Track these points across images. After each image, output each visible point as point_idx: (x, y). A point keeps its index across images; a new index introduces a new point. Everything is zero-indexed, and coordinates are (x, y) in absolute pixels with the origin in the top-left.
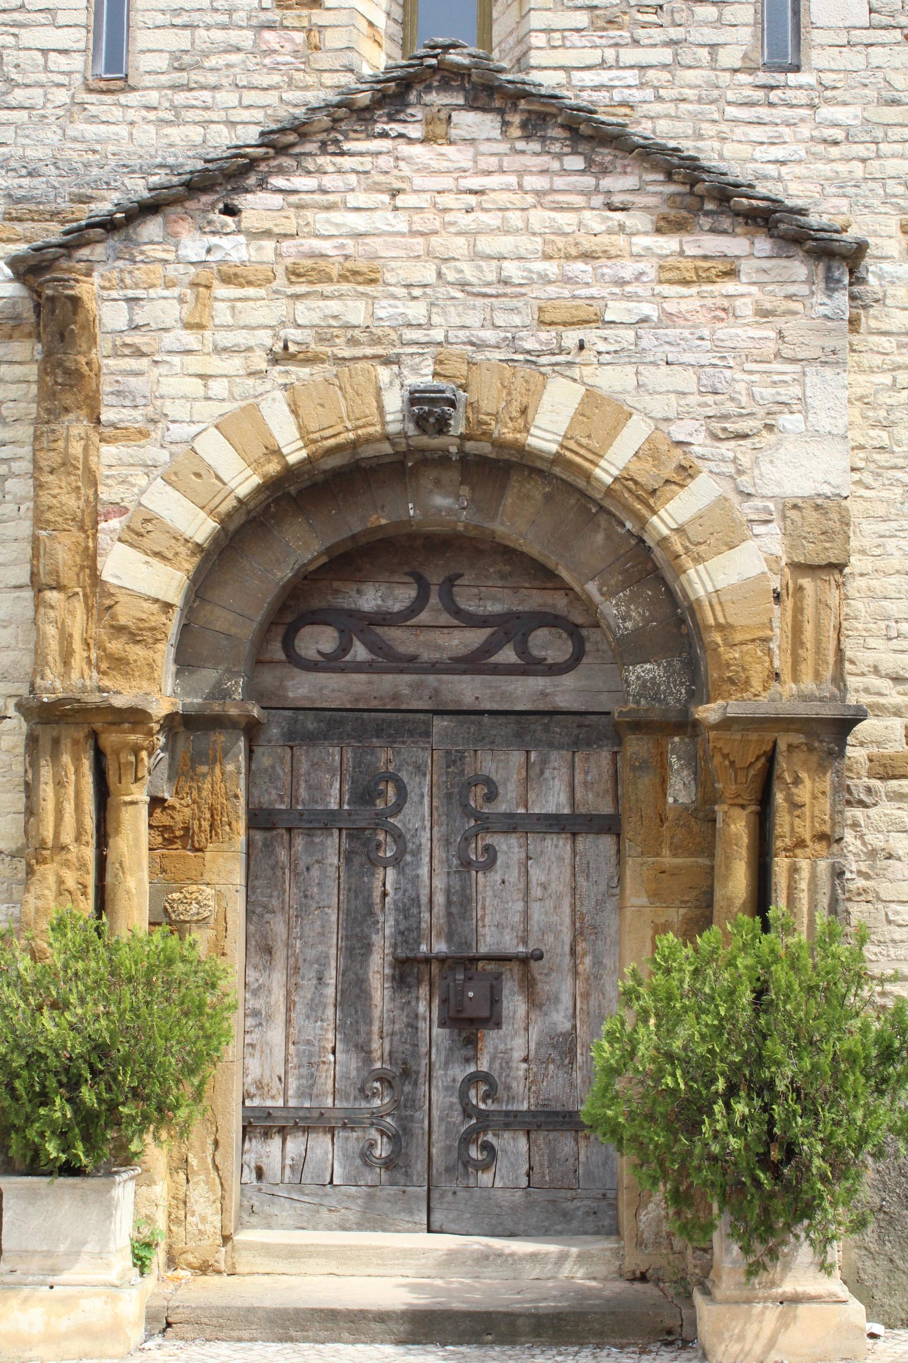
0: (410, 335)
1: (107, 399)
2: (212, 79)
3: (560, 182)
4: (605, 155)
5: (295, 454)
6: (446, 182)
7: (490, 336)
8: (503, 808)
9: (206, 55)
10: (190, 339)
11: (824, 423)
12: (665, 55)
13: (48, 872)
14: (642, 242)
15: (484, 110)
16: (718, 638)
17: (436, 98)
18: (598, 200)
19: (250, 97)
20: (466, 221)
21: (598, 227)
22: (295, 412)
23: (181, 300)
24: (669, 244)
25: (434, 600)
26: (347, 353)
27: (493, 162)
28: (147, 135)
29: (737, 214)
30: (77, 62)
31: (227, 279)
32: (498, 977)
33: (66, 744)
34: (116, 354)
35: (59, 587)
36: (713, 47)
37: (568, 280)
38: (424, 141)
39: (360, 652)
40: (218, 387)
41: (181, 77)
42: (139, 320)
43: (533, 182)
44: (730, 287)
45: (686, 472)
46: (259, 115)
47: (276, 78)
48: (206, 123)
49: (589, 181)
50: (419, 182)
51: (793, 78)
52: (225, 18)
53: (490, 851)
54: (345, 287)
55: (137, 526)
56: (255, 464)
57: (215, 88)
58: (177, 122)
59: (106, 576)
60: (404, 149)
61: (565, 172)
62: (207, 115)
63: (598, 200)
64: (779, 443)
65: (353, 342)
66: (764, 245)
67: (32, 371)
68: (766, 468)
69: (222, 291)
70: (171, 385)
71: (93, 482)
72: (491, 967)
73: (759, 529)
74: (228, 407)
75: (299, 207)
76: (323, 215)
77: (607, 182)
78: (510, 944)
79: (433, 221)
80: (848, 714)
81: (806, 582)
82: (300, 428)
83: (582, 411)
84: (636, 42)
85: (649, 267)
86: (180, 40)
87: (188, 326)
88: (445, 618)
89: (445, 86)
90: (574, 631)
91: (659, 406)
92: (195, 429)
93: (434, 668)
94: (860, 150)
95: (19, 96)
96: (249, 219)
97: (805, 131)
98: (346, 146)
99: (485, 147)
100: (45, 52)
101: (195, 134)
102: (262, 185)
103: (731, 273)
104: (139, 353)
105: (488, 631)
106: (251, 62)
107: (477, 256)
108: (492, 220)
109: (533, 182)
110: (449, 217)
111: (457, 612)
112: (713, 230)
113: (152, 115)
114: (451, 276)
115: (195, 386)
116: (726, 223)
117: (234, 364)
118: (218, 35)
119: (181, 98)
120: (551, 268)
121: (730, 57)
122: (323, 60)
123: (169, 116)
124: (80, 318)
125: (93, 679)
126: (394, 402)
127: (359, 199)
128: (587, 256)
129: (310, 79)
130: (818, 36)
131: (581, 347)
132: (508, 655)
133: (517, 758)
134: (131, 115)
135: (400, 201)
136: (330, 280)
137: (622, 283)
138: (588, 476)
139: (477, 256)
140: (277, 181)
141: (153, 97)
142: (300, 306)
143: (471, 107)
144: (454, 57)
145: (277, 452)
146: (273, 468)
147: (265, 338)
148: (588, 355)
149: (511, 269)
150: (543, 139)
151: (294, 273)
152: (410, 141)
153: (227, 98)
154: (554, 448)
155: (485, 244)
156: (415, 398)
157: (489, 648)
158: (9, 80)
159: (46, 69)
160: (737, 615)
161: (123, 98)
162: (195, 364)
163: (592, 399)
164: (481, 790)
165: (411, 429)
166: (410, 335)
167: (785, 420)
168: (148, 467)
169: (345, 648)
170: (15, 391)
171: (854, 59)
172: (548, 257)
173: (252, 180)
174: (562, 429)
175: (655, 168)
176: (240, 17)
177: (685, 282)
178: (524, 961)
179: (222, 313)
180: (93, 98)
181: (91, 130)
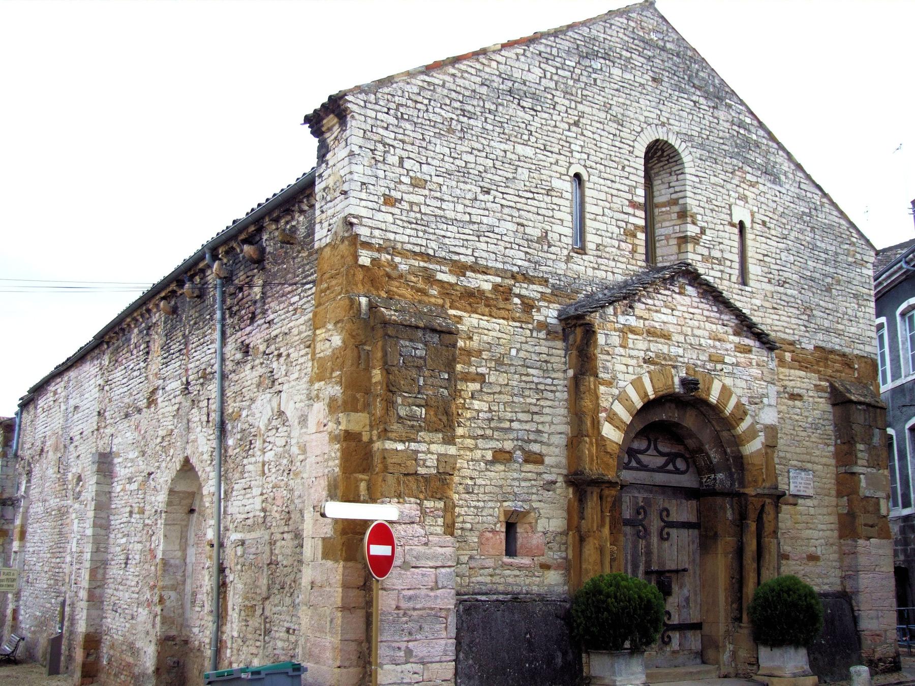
0: (680, 359)
1: (601, 369)
2: (607, 256)
3: (712, 314)
4: (722, 307)
5: (652, 397)
6: (685, 309)
7: (699, 363)
8: (670, 519)
9: (606, 247)
10: (621, 351)
11: (773, 402)
12: (719, 274)
13: (591, 539)
14: (732, 338)
15: (693, 286)
16: (750, 467)
17: (682, 280)
18: (721, 322)
19: (619, 265)
20: (691, 323)
21: (721, 331)
22: (651, 381)
23: (619, 336)
24: (736, 339)
25: (652, 446)
26: (663, 362)
27: (695, 304)
28: (590, 272)
29: (752, 332)
30: (569, 240)
31: (633, 331)
32: (670, 578)
33: (595, 494)
34: (601, 353)
35: (587, 436)
36: (730, 275)
37: (714, 347)
38: (680, 293)
39: (634, 464)
40: (631, 369)
41: (599, 253)
42: (609, 342)
43: (706, 313)
44: (751, 356)
45: (745, 413)
46: (620, 271)
47: (624, 260)
48: (606, 271)
49: (718, 315)
50: (679, 307)
51: (747, 288)
52: (610, 235)
53: (668, 534)
54: (662, 340)
55: (611, 416)
56: (642, 399)
57: (609, 259)
58: (598, 269)
59: (603, 433)
60: (675, 295)
61: (712, 311)
62: (606, 268)
63: (721, 322)
64: (763, 408)
65: (665, 359)
66: (757, 344)
67: (562, 353)
68: (761, 414)
69: (630, 336)
70: (620, 368)
71: (597, 398)
72: (667, 575)
73: (760, 434)
74: (634, 377)
75: (649, 310)
76: (655, 314)
77: (723, 317)
78: (674, 567)
79: (681, 322)
80: (780, 494)
81: (769, 451)
82: (653, 386)
83: (721, 392)
84: (712, 269)
85: (732, 346)
86: (598, 240)
87: (621, 346)
88: (655, 453)
89: (683, 277)
90: (686, 460)
91: (739, 392)
92: (625, 383)
93: (653, 470)
94: (761, 314)
95: (553, 249)
96: (637, 312)
97: (750, 306)
98: (662, 291)
99: (694, 299)
100: (560, 235)
101: (603, 274)
102: (639, 300)
103: (750, 351)
104: (608, 354)
105: (666, 458)
106: (618, 252)
107: (694, 335)
108: (696, 323)
109: (706, 313)
110: (688, 321)
111: (658, 451)
112: (747, 337)
113: (591, 265)
114: (688, 341)
115: (623, 368)
116: (749, 335)
117: (633, 362)
118: (609, 240)
119: (600, 261)
120: (711, 342)
121: (734, 278)
122: (637, 256)
123: (596, 266)
124: (593, 339)
125: (601, 471)
126: (677, 380)
127: (664, 310)
128: (719, 340)
129: (634, 262)
130: (751, 276)
131: (722, 370)
132: (670, 467)
133: (674, 502)
134: (586, 264)
135: (675, 313)
136: (658, 337)
137: (727, 350)
138: (723, 412)
139: (694, 335)
140: (643, 300)
141: (592, 259)
142: (652, 344)
143: (690, 285)
144: (690, 268)
145: (646, 395)
146: (646, 400)
147: (642, 354)
148: (722, 373)
149: (702, 341)
150: (707, 299)
151: (649, 333)
152: (676, 293)
153: (612, 264)
154: (715, 402)
155: (697, 332)
156: (684, 382)
157: (666, 464)
158: (549, 243)
159: (560, 241)
160: (757, 461)
161: (584, 257)
162: (625, 360)
163: (724, 388)
164: (665, 513)
165: (682, 391)
166: (680, 359)
167: (765, 400)
168: (613, 396)
169: (630, 461)
170: (557, 359)
171: (758, 285)
172: (710, 339)
173: (637, 298)
174: (717, 396)
175: (733, 314)
176: (615, 236)
177: (741, 352)
178: (677, 572)
179: (630, 341)
180: (575, 255)
181: (575, 267)
